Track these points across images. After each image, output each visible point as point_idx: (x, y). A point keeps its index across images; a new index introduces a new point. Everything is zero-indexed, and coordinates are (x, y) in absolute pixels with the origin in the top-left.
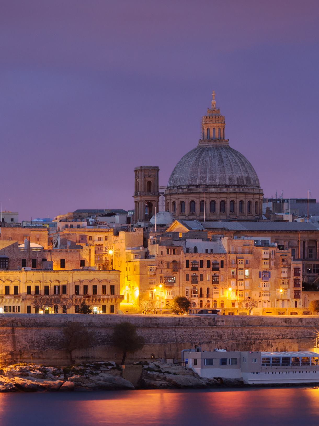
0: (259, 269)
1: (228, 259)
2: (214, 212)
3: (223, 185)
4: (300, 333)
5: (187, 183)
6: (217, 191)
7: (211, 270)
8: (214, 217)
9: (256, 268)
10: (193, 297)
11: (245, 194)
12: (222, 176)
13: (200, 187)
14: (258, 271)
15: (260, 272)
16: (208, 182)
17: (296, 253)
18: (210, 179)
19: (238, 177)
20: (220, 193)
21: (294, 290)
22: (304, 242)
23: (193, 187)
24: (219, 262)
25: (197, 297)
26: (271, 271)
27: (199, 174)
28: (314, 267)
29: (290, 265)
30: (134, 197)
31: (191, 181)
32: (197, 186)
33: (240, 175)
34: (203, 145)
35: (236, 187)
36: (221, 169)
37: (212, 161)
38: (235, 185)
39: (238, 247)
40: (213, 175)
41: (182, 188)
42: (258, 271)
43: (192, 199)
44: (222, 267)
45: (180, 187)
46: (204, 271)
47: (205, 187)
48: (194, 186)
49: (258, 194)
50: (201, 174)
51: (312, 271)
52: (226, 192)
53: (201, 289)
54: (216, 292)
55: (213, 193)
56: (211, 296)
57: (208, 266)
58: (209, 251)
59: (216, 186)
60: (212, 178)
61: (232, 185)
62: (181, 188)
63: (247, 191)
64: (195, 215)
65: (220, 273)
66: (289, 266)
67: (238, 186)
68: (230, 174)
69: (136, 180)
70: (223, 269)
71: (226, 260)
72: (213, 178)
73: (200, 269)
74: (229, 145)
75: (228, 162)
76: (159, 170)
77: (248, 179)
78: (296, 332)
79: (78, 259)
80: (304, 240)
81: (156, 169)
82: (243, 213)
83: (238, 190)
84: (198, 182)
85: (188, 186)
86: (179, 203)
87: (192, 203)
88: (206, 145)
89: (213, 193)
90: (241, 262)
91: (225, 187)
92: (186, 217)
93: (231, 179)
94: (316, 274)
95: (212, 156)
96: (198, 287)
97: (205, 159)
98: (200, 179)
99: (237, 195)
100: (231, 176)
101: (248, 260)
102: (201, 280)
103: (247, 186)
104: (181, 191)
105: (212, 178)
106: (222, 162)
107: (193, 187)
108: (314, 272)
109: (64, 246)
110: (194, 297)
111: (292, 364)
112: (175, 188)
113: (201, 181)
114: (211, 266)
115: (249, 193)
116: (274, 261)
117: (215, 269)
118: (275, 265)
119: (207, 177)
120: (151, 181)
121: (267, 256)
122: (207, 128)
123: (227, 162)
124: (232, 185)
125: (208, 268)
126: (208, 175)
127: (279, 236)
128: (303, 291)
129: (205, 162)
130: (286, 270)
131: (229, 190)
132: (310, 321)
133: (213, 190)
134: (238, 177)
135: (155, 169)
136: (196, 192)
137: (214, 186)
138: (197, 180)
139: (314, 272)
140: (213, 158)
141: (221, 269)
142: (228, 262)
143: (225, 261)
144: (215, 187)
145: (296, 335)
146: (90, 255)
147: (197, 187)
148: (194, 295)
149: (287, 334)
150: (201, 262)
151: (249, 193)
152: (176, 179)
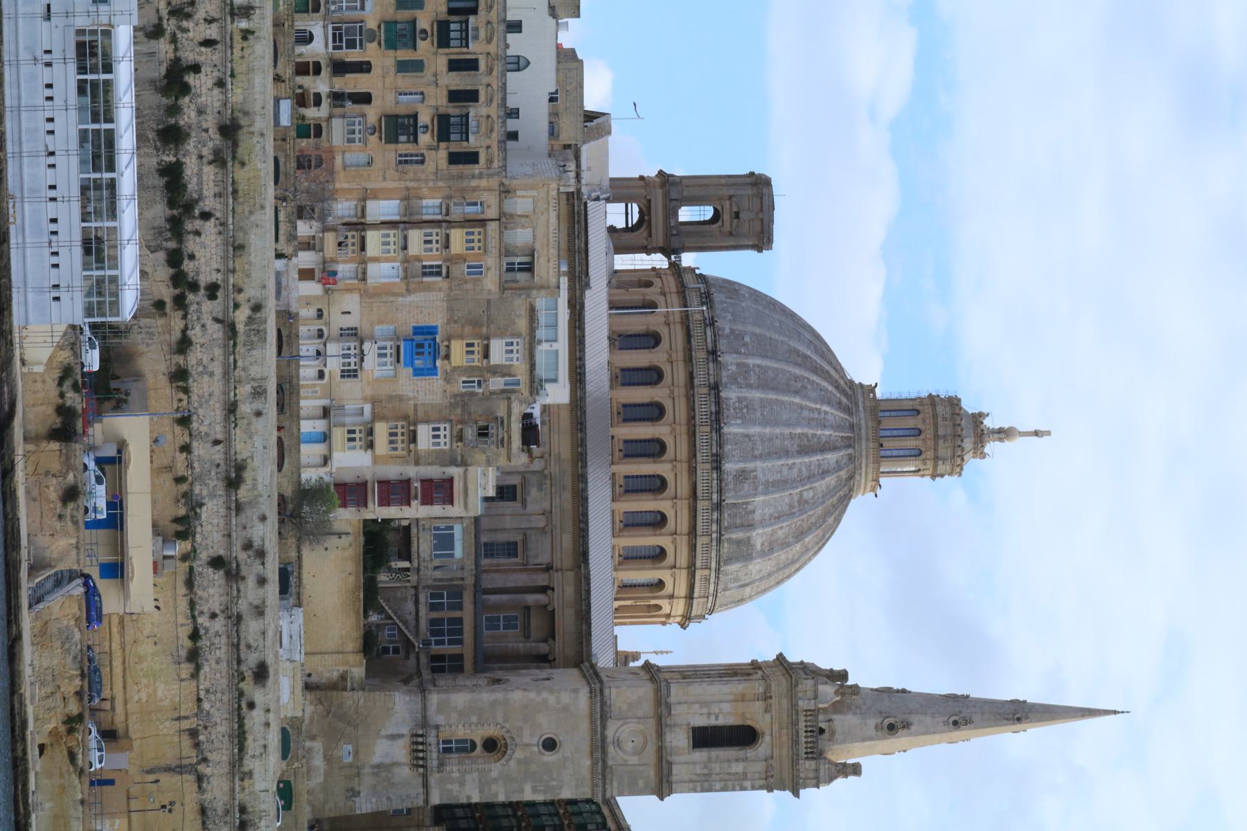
0: (449, 323)
1: (483, 183)
2: (620, 419)
3: (720, 445)
4: (206, 388)
5: (725, 325)
6: (697, 422)
7: (442, 111)
9: (450, 310)
10: (334, 28)
11: (689, 534)
12: (755, 444)
13: (711, 365)
14: (438, 319)
15: (436, 327)
16: (730, 394)
17: (502, 561)
18: (740, 400)
19: (750, 507)
20: (692, 435)
21: (366, 482)
22: (544, 589)
23: (709, 340)
24: (474, 142)
25: (335, 48)
26: (437, 383)
28: (453, 621)
29: (464, 463)
30: (661, 173)
32: (713, 353)
33: (757, 516)
35: (715, 496)
36: (778, 442)
37: (805, 413)
38: (720, 491)
39: (530, 230)
40: (755, 410)
44: (454, 159)
46: (435, 75)
47: (712, 381)
48: (715, 342)
49: (691, 587)
50: (757, 370)
51: (435, 615)
52: (695, 456)
53: (364, 67)
54: (353, 132)
55: (691, 408)
56: (338, 111)
57: (455, 96)
58: (512, 125)
59: (718, 421)
60: (747, 407)
61: (720, 480)
63: (701, 541)
65: (430, 148)
66: (459, 458)
67: (719, 507)
68: (760, 475)
70: (443, 163)
71: (481, 176)
73: (442, 62)
75: (805, 473)
77: (744, 552)
78: (210, 369)
80: (553, 589)
81: (762, 239)
82: (621, 530)
83: (701, 505)
84: (728, 359)
86: (648, 298)
89: (691, 408)
90: (473, 241)
91: (713, 455)
93: (742, 475)
94: (423, 624)
95: (822, 416)
96: (370, 52)
97: (809, 387)
98: (738, 365)
99: (686, 502)
100: (756, 477)
101: (481, 273)
102: (403, 67)
103: (719, 541)
105: (747, 407)
106: (804, 451)
107: (709, 340)
108: (433, 622)
110: (334, 35)
111: (85, 81)
113: (734, 368)
114: (453, 110)
115: (693, 548)
116: (480, 391)
117: (445, 127)
118: (463, 395)
120: (720, 223)
123: (804, 469)
124: (720, 480)
125: (445, 93)
126: (757, 395)
127: (564, 488)
128: (366, 523)
129: (800, 385)
130: (445, 444)
131: (703, 469)
132: (255, 438)
133: (704, 408)
134: (750, 507)
135: (762, 232)
137: (718, 413)
139: (433, 622)
140: (816, 416)
141: (442, 154)
142: (474, 183)
143: (476, 169)
144: (713, 418)
145: (200, 369)
147: (709, 352)
148: (341, 35)
149: (203, 326)
150: (472, 65)
151: (693, 548)
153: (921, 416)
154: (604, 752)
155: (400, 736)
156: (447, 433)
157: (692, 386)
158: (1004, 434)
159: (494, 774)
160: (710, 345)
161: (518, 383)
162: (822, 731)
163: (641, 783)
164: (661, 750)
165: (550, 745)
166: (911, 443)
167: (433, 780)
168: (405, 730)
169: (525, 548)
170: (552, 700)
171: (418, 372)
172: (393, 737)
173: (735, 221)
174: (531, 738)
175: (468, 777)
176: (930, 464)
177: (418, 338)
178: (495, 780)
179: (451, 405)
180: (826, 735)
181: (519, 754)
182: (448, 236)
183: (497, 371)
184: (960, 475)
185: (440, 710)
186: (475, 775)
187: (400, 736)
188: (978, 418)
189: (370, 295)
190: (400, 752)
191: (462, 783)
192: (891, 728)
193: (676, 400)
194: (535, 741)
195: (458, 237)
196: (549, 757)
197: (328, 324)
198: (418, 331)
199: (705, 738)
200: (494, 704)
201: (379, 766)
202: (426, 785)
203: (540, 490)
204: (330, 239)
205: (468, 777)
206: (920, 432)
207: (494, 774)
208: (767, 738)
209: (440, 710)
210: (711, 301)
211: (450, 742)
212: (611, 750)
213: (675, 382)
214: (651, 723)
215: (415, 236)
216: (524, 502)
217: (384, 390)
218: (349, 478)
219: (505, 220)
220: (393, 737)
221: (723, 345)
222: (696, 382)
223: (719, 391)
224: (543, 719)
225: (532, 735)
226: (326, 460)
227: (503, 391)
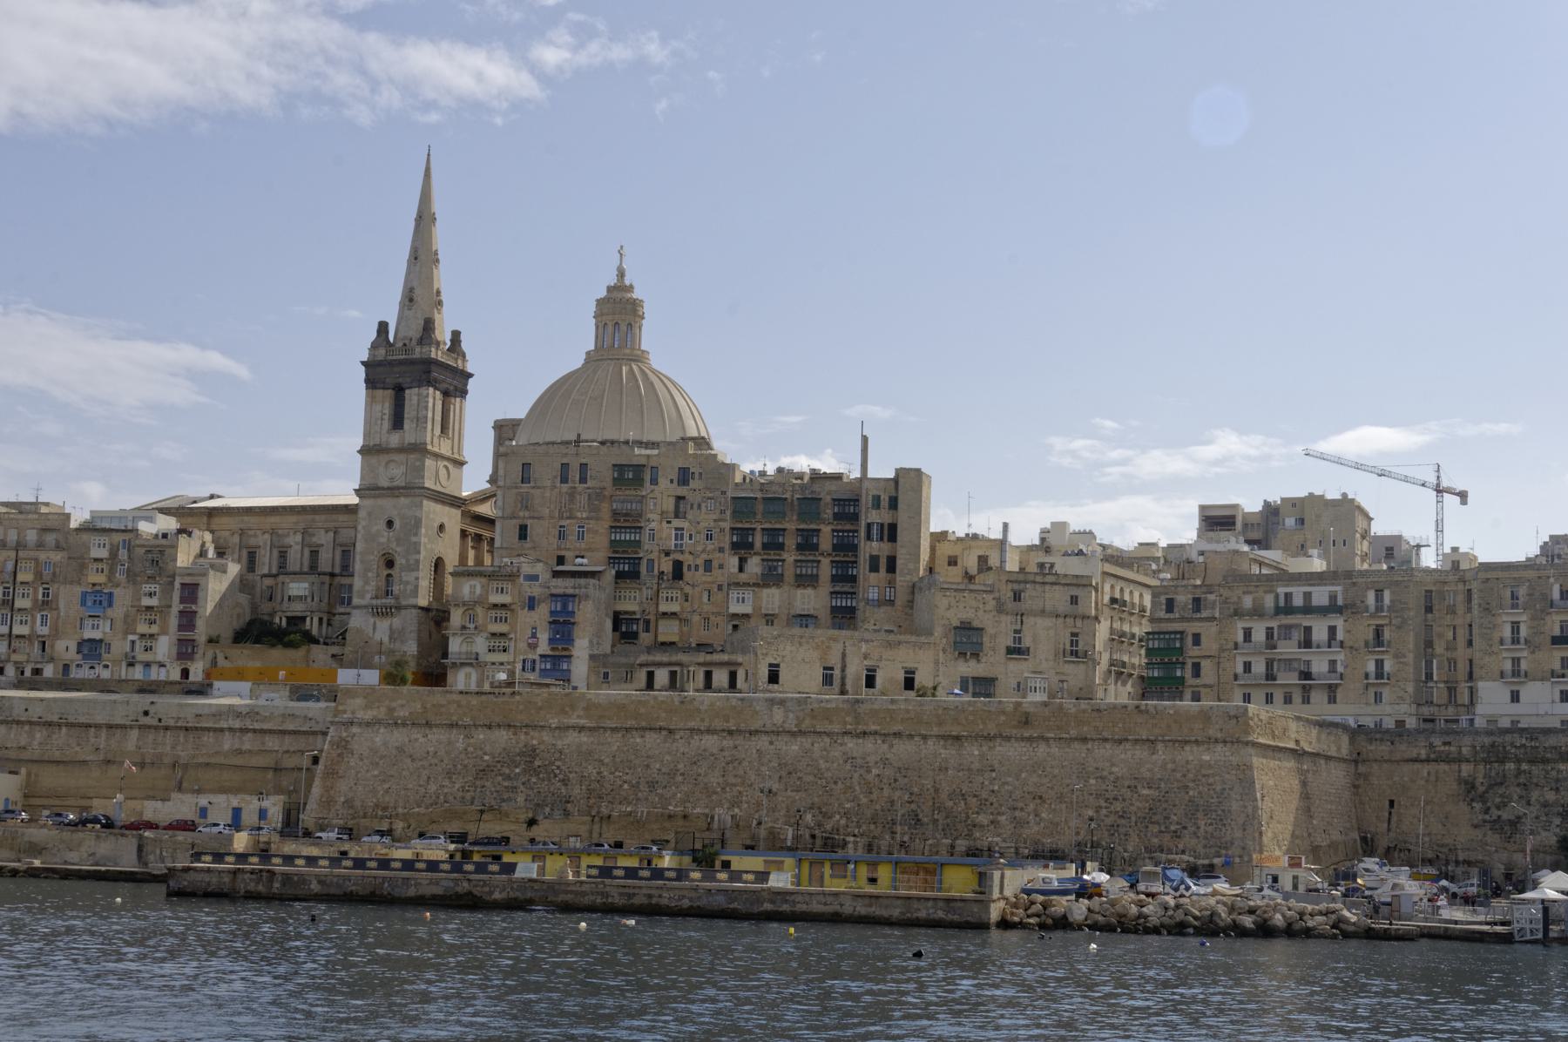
0: (80, 584)
9: (71, 583)
14: (78, 590)
26: (116, 591)
29: (173, 576)
39: (28, 531)
42: (78, 590)
121: (103, 553)
154: (398, 488)
155: (375, 623)
156: (148, 586)
158: (621, 274)
159: (404, 561)
161: (124, 541)
162: (405, 345)
163: (418, 463)
164: (402, 450)
165: (390, 524)
166: (623, 327)
167: (404, 603)
168: (372, 620)
169: (346, 545)
170: (363, 523)
171: (110, 605)
172: (374, 629)
174: (385, 536)
175: (404, 579)
176: (637, 319)
177: (89, 603)
178: (408, 560)
179: (134, 584)
180: (407, 342)
181: (394, 545)
182: (22, 583)
183: (114, 554)
185: (362, 597)
186: (403, 574)
187: (375, 623)
188: (610, 289)
189: (56, 633)
190: (384, 625)
191: (407, 583)
192: (411, 300)
194: (386, 534)
195: (21, 577)
196: (397, 524)
197: (72, 661)
198: (83, 603)
199: (397, 422)
200: (362, 562)
201: (390, 638)
202: (406, 607)
203: (314, 535)
204: (15, 657)
205: (404, 579)
206: (617, 323)
207: (404, 561)
208: (400, 380)
209: (362, 597)
211: (388, 591)
212: (395, 484)
214: (384, 458)
215: (19, 603)
216: (323, 545)
217: (119, 625)
218: (174, 651)
219: (20, 546)
220: (374, 629)
224: (375, 529)
225: (383, 536)
226: (162, 665)
227: (129, 550)
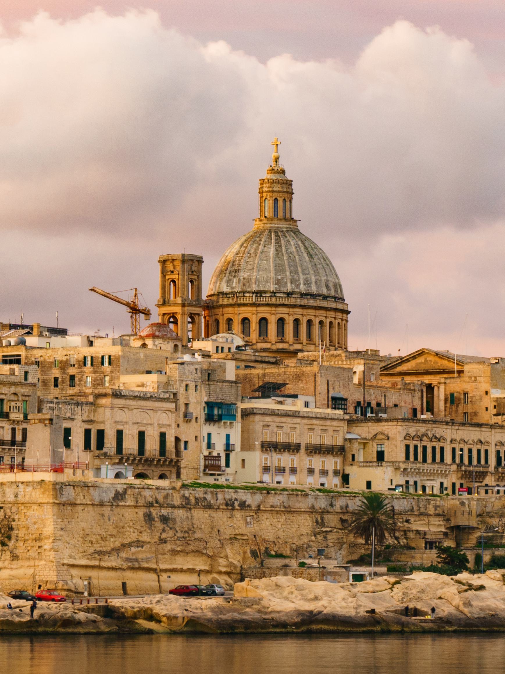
5: (272, 288)
8: (298, 347)
13: (293, 296)
16: (303, 288)
18: (305, 284)
23: (282, 295)
27: (288, 273)
31: (278, 285)
34: (271, 225)
41: (264, 295)
43: (280, 315)
45: (259, 293)
47: (299, 296)
48: (284, 293)
50: (292, 275)
62: (261, 296)
64: (286, 342)
69: (165, 276)
72: (307, 283)
74: (298, 228)
76: (203, 262)
79: (410, 406)
85: (275, 293)
87: (263, 322)
88: (276, 226)
92: (273, 344)
104: (263, 301)
107: (282, 295)
109: (261, 384)
112: (245, 295)
113: (293, 285)
119: (301, 279)
122: (274, 198)
126: (302, 277)
129: (291, 255)
136: (289, 303)
138: (287, 283)
146: (422, 400)
147: (288, 296)
152: (249, 280)
153: (279, 199)
157: (305, 306)
160: (285, 295)
173: (195, 273)
184: (292, 181)
193: (278, 312)
210: (261, 291)
213: (287, 312)
221: (283, 289)
222: (302, 304)
223: (304, 293)
